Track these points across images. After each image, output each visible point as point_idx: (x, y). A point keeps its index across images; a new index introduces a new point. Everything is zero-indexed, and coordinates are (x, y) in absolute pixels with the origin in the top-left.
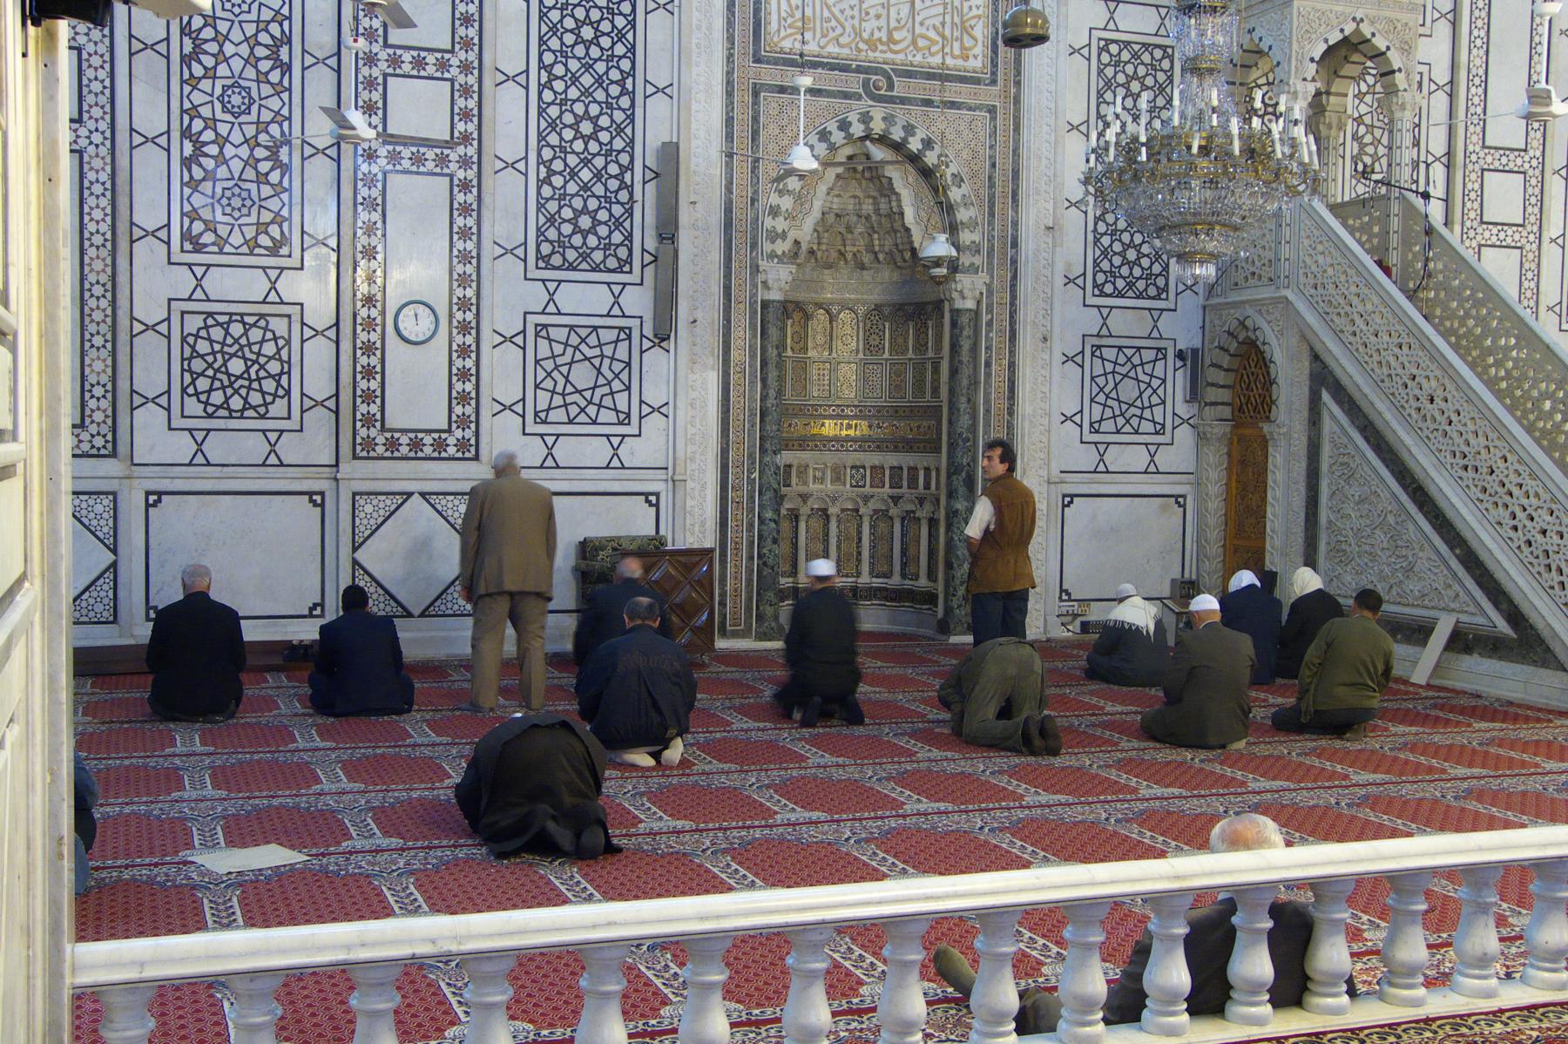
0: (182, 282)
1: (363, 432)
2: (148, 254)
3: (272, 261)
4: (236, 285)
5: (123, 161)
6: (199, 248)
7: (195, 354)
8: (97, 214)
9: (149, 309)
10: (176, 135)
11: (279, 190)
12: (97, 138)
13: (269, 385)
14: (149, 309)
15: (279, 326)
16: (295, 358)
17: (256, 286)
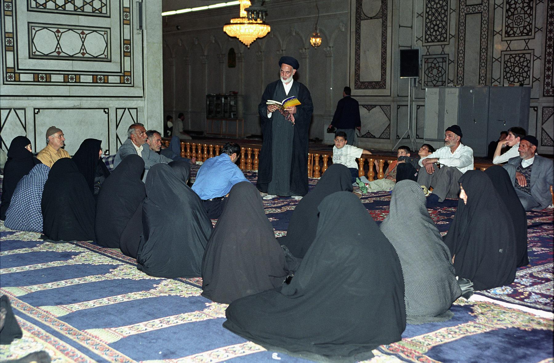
0: (504, 46)
1: (546, 88)
2: (497, 38)
3: (527, 37)
4: (518, 45)
5: (491, 14)
6: (509, 36)
7: (507, 67)
8: (484, 29)
9: (497, 55)
10: (505, 3)
11: (530, 15)
12: (485, 8)
13: (525, 75)
14: (497, 55)
15: (527, 56)
16: (532, 66)
17: (522, 45)
